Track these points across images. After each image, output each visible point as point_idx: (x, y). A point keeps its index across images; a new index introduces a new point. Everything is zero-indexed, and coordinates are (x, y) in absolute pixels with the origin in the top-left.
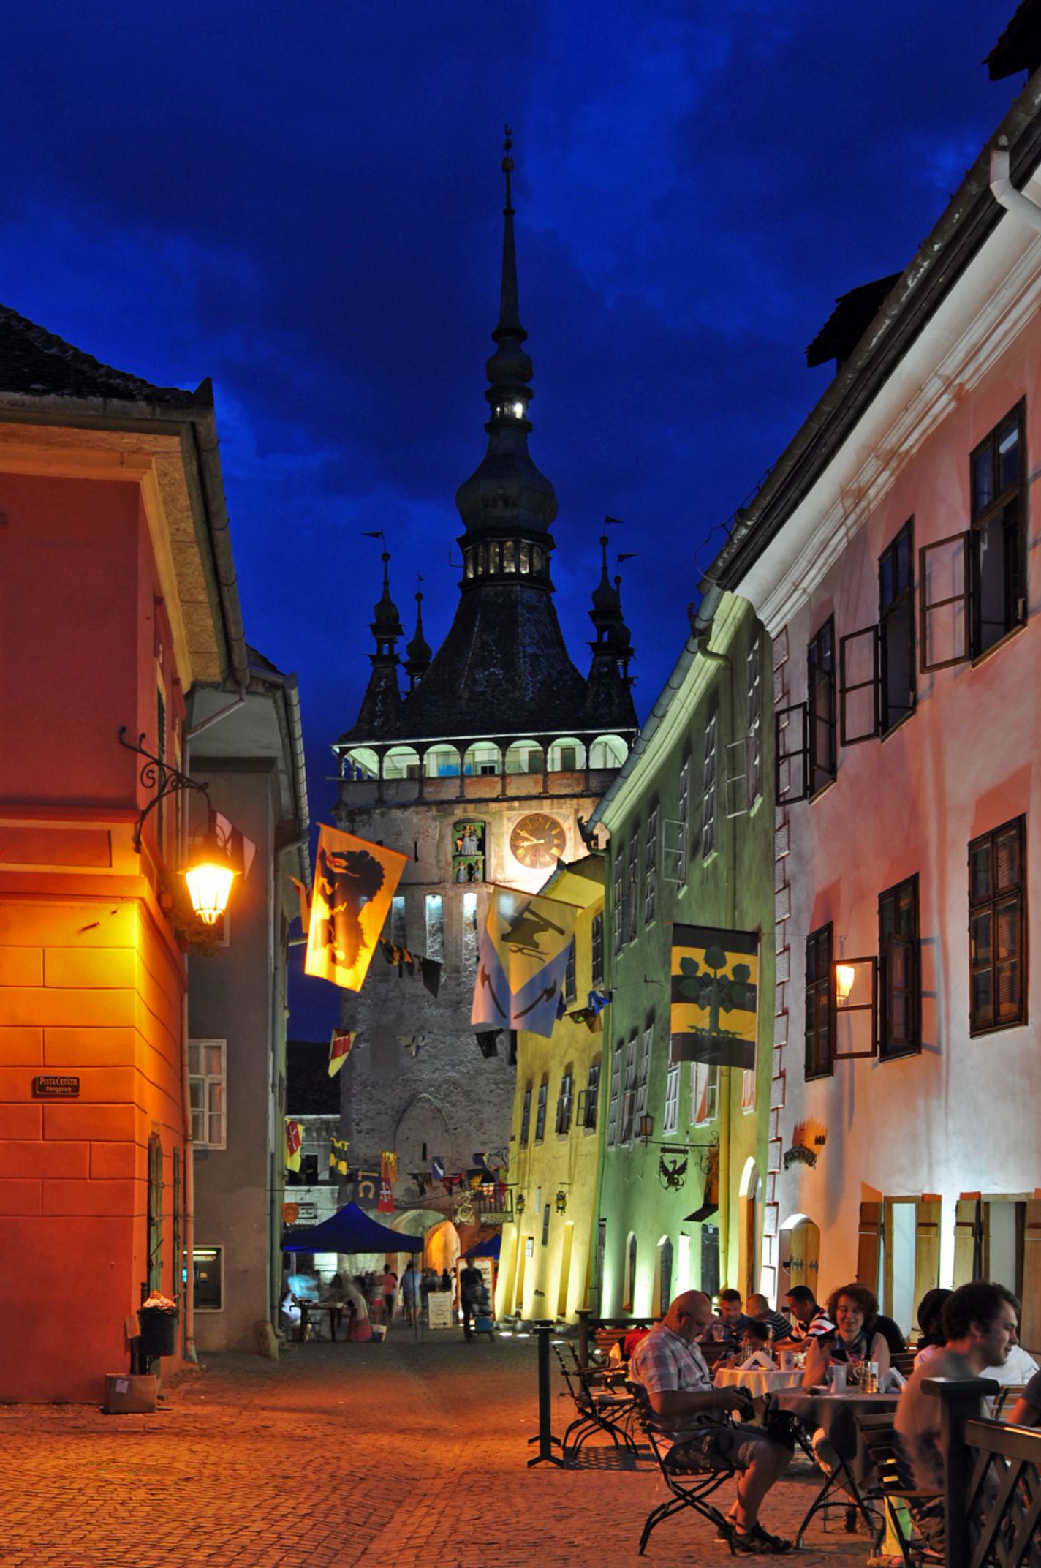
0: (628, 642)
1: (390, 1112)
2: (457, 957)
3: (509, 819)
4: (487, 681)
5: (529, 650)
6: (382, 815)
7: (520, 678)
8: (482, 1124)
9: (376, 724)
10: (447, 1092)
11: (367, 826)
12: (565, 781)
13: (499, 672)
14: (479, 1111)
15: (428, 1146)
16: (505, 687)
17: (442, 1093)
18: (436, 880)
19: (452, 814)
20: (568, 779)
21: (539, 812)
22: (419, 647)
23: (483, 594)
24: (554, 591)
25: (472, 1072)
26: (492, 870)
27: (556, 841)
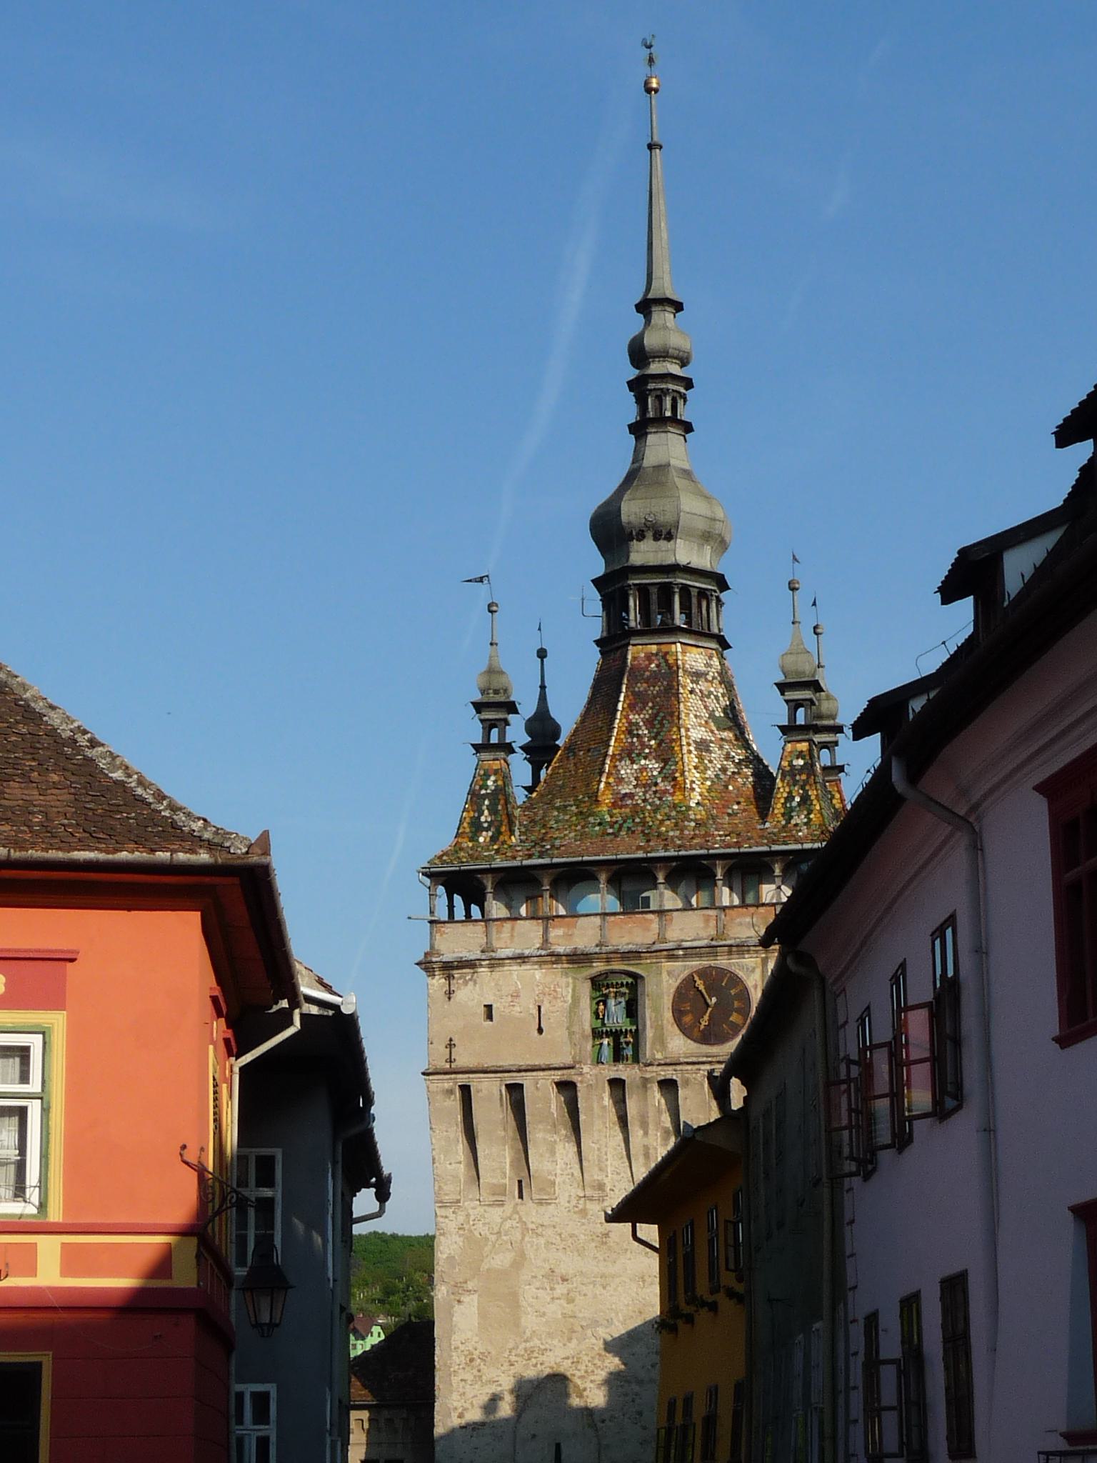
0: (833, 717)
2: (601, 1170)
3: (669, 973)
4: (636, 779)
5: (697, 734)
6: (491, 966)
7: (682, 774)
8: (640, 1414)
9: (481, 839)
10: (591, 1368)
11: (471, 983)
13: (654, 765)
14: (637, 1394)
16: (662, 786)
18: (568, 1061)
19: (593, 967)
21: (712, 963)
22: (542, 727)
23: (629, 657)
24: (729, 647)
26: (648, 1046)
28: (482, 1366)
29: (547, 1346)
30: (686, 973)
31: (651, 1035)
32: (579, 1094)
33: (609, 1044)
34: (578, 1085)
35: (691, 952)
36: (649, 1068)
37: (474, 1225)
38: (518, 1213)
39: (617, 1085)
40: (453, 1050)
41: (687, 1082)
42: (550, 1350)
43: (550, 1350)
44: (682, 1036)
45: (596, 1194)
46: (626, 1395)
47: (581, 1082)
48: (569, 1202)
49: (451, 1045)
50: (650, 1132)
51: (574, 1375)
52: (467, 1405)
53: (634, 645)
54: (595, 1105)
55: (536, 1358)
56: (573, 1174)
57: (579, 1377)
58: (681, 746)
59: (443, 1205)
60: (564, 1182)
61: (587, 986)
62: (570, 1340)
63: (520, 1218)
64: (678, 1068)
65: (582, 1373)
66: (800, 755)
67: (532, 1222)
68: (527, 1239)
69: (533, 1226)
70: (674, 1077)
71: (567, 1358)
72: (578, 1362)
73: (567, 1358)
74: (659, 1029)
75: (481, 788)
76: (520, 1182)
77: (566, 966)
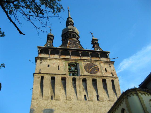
2: (70, 95)
3: (83, 63)
18: (65, 74)
30: (86, 64)
34: (67, 78)
35: (87, 60)
36: (81, 76)
37: (40, 104)
38: (51, 102)
39: (74, 80)
40: (41, 71)
44: (87, 72)
47: (67, 77)
48: (63, 100)
49: (40, 70)
50: (81, 88)
54: (70, 82)
56: (64, 95)
59: (34, 99)
60: (62, 97)
61: (67, 65)
63: (52, 103)
64: (87, 77)
67: (54, 104)
69: (54, 105)
74: (82, 71)
76: (52, 96)
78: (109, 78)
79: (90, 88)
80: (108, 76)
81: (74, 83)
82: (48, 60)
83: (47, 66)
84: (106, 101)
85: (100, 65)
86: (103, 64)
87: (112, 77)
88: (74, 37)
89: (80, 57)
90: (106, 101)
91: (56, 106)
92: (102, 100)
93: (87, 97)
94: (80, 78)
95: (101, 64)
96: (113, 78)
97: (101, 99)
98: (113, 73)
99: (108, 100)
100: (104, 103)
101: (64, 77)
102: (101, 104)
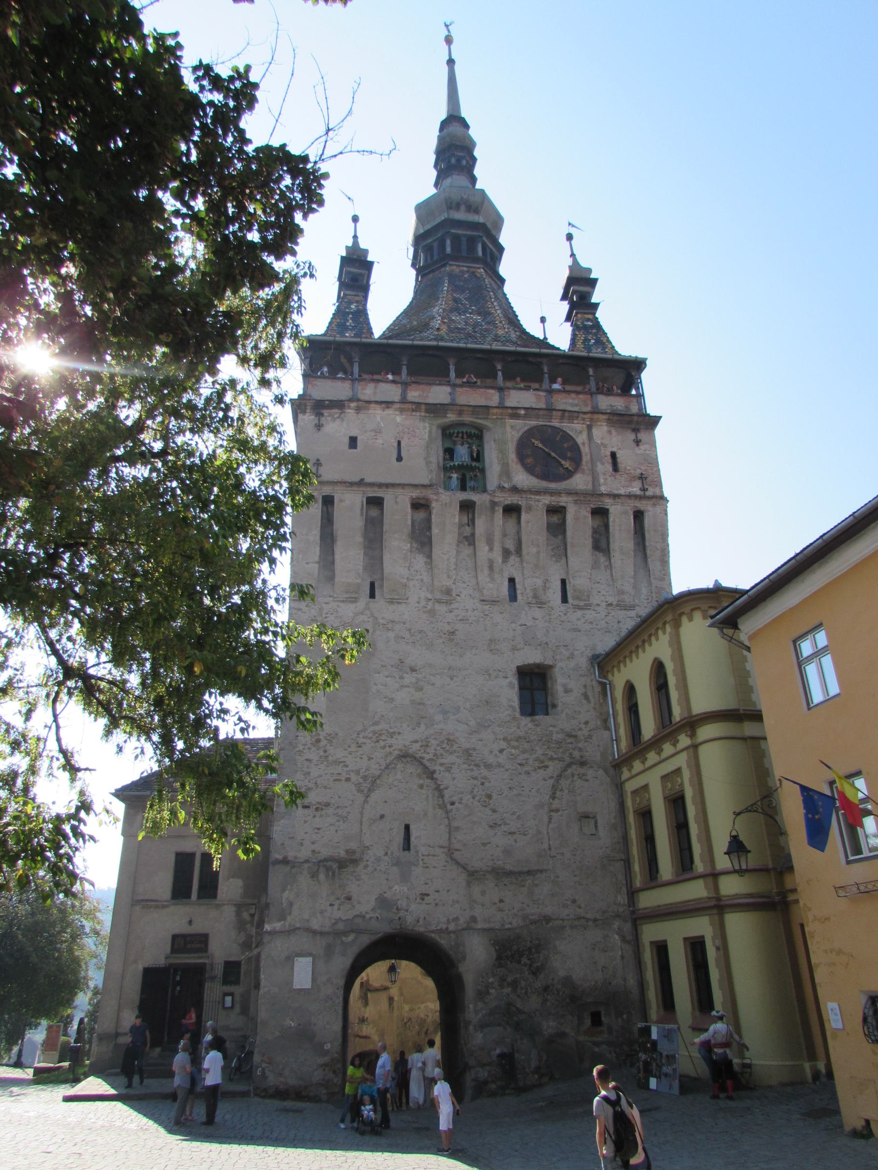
1: (354, 777)
2: (449, 577)
3: (512, 427)
4: (466, 322)
6: (358, 410)
8: (489, 797)
10: (440, 751)
11: (338, 422)
12: (571, 401)
14: (485, 778)
15: (412, 827)
17: (431, 750)
18: (426, 482)
19: (446, 417)
20: (573, 399)
25: (472, 723)
27: (569, 454)
28: (328, 747)
29: (396, 730)
30: (526, 428)
31: (499, 469)
32: (434, 512)
33: (457, 479)
38: (369, 609)
39: (467, 507)
41: (529, 509)
42: (399, 733)
43: (399, 733)
45: (445, 598)
46: (475, 778)
48: (418, 602)
50: (495, 548)
51: (423, 758)
52: (311, 785)
53: (451, 265)
55: (384, 740)
56: (422, 580)
57: (428, 760)
58: (496, 310)
60: (414, 586)
62: (419, 724)
63: (372, 615)
65: (431, 756)
66: (588, 320)
67: (383, 618)
68: (378, 633)
69: (382, 621)
70: (520, 503)
71: (416, 742)
72: (427, 746)
73: (416, 742)
75: (346, 308)
76: (372, 585)
77: (423, 414)
78: (623, 504)
79: (535, 550)
80: (622, 491)
81: (469, 525)
82: (350, 412)
83: (346, 440)
84: (598, 605)
85: (590, 437)
86: (605, 428)
87: (636, 497)
88: (476, 260)
89: (501, 390)
90: (598, 605)
91: (390, 626)
92: (582, 603)
93: (518, 586)
94: (494, 504)
95: (596, 432)
96: (644, 502)
97: (580, 600)
98: (646, 478)
99: (611, 605)
100: (590, 614)
101: (424, 498)
102: (578, 619)
